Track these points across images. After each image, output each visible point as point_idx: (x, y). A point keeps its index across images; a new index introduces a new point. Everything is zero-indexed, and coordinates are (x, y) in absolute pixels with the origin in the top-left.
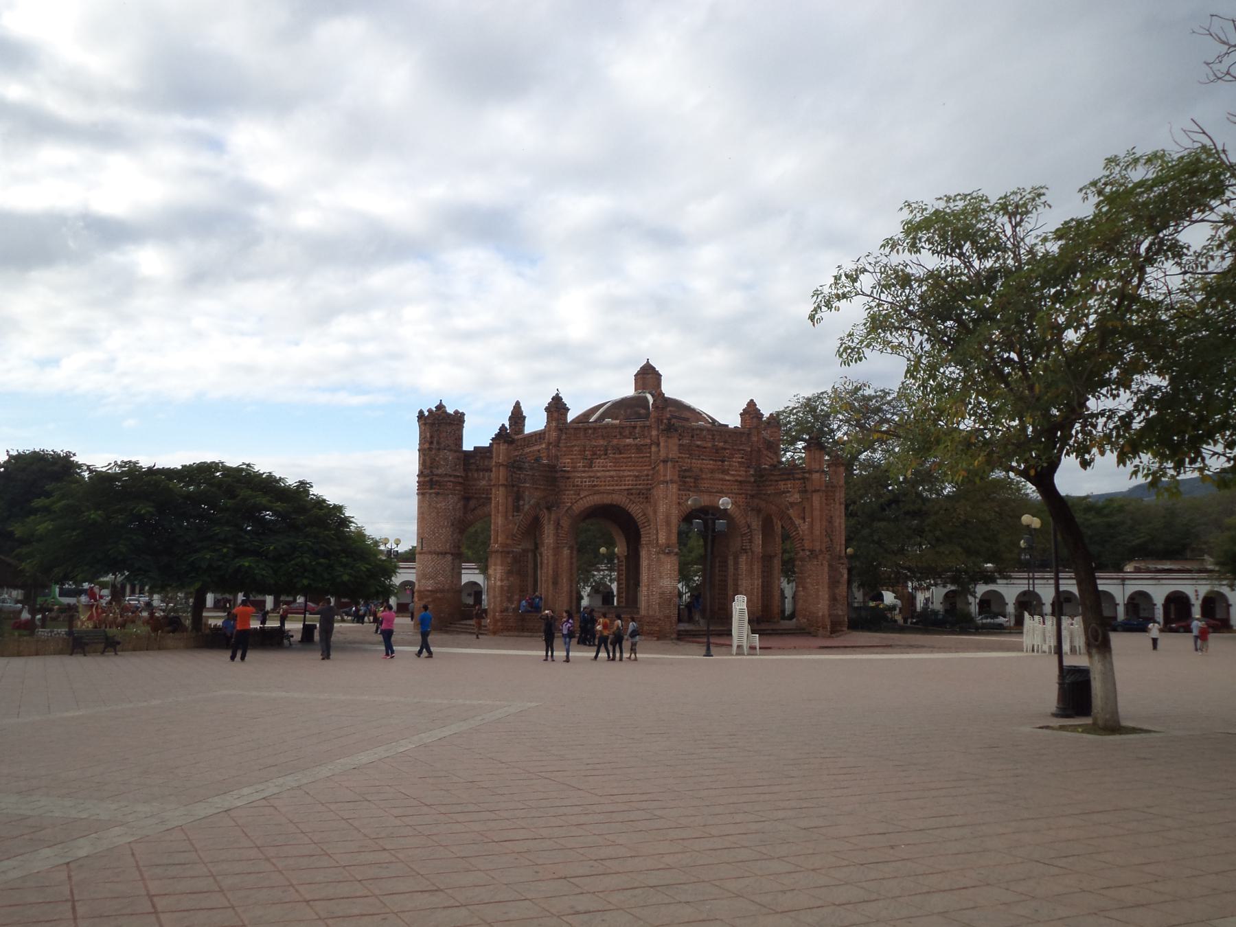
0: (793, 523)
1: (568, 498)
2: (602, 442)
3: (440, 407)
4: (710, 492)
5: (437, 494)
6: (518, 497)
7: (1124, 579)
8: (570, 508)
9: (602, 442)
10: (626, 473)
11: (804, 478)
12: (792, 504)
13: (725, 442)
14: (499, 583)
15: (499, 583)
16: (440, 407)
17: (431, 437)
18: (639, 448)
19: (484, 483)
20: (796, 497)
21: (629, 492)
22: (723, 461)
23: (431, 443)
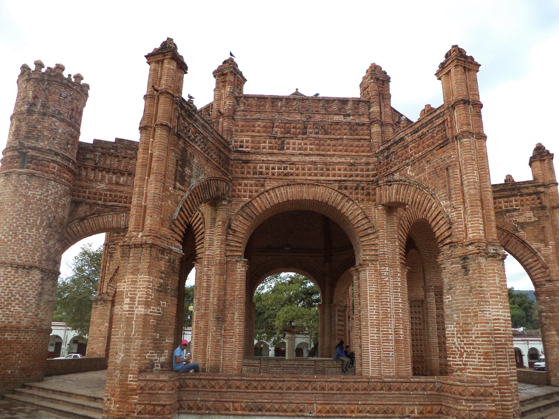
1: (246, 189)
2: (298, 117)
5: (32, 175)
6: (183, 161)
7: (528, 341)
8: (247, 205)
9: (298, 117)
10: (335, 160)
11: (537, 193)
12: (523, 225)
14: (140, 310)
15: (140, 310)
17: (35, 97)
18: (353, 128)
19: (103, 186)
20: (529, 216)
21: (342, 185)
23: (33, 105)
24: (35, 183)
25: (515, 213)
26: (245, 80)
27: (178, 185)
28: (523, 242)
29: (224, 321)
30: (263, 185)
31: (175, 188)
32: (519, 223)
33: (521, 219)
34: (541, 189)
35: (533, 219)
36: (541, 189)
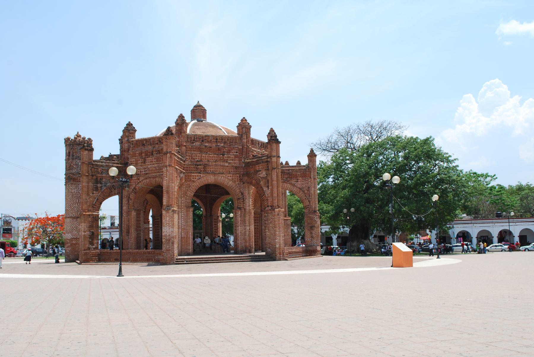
0: (263, 190)
3: (78, 136)
4: (214, 173)
8: (135, 188)
9: (150, 147)
13: (225, 143)
16: (78, 136)
20: (263, 174)
22: (223, 155)
24: (74, 186)
25: (260, 173)
26: (135, 131)
27: (95, 192)
28: (262, 187)
29: (129, 233)
30: (139, 179)
31: (93, 193)
32: (261, 178)
33: (261, 176)
34: (269, 160)
35: (266, 175)
36: (269, 160)
